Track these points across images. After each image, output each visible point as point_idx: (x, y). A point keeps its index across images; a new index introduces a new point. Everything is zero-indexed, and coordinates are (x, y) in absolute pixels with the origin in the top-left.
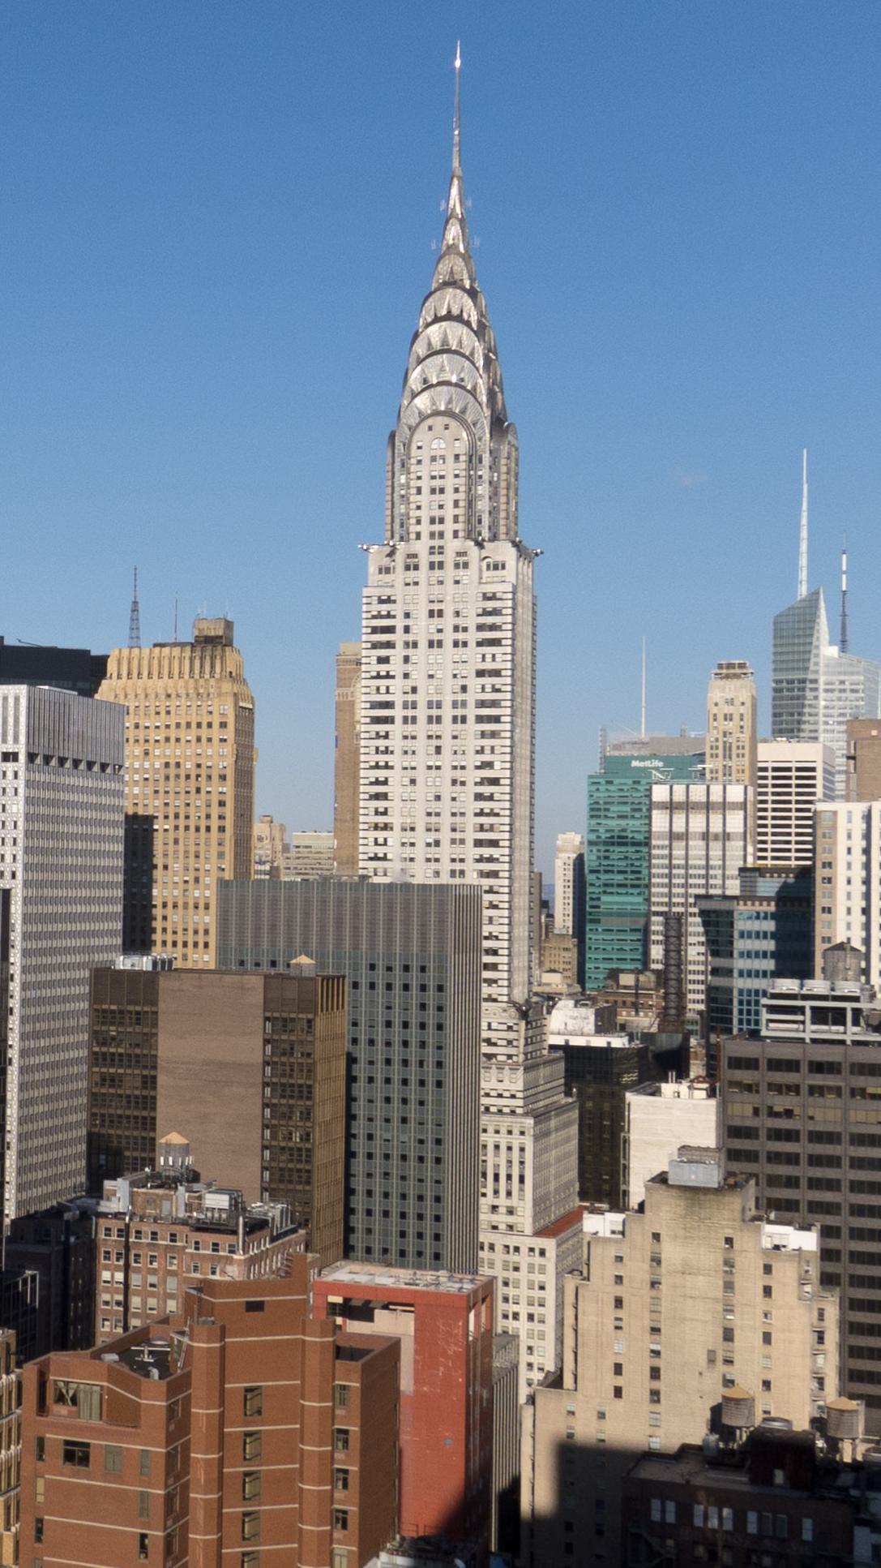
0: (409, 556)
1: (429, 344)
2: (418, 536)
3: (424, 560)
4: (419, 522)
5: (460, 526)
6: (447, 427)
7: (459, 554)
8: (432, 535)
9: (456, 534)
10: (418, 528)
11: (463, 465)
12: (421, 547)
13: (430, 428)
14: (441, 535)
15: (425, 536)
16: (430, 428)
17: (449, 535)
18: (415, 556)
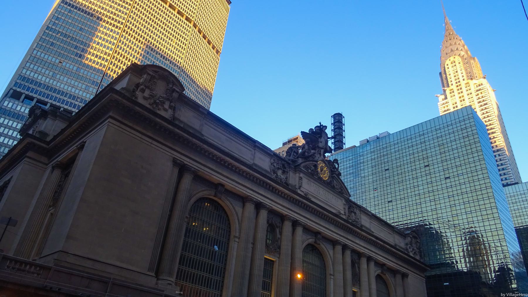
2: (452, 85)
3: (455, 89)
5: (465, 77)
7: (466, 84)
9: (464, 80)
12: (454, 87)
14: (459, 82)
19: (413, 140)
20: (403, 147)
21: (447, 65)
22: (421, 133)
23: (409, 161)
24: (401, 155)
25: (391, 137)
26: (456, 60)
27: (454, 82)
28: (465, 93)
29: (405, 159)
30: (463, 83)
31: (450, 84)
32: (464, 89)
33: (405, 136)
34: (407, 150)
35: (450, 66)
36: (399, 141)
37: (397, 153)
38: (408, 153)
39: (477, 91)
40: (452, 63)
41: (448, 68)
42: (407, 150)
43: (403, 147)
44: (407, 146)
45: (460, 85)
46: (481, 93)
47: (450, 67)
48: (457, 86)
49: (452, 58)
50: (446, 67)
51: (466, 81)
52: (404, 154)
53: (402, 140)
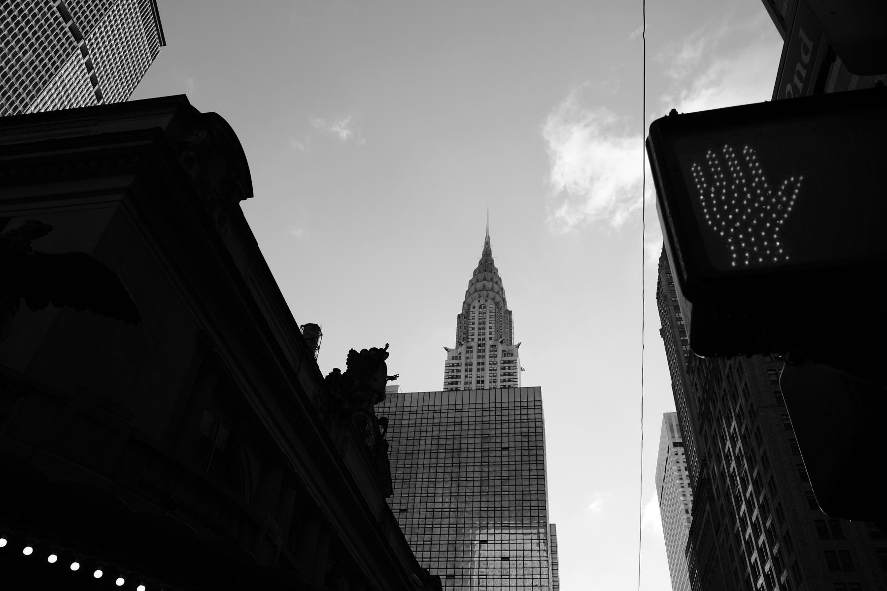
2: (473, 340)
7: (491, 346)
8: (479, 340)
12: (474, 344)
14: (484, 339)
15: (476, 340)
17: (487, 339)
19: (443, 415)
20: (424, 421)
21: (474, 307)
22: (458, 407)
23: (428, 447)
24: (417, 434)
25: (408, 399)
27: (476, 337)
28: (487, 360)
29: (422, 442)
30: (489, 343)
32: (487, 353)
33: (432, 403)
34: (430, 429)
35: (477, 310)
36: (420, 409)
37: (412, 429)
38: (429, 434)
39: (505, 362)
40: (480, 307)
42: (430, 429)
43: (424, 421)
44: (430, 421)
45: (483, 345)
46: (509, 368)
51: (491, 343)
52: (423, 434)
53: (426, 408)
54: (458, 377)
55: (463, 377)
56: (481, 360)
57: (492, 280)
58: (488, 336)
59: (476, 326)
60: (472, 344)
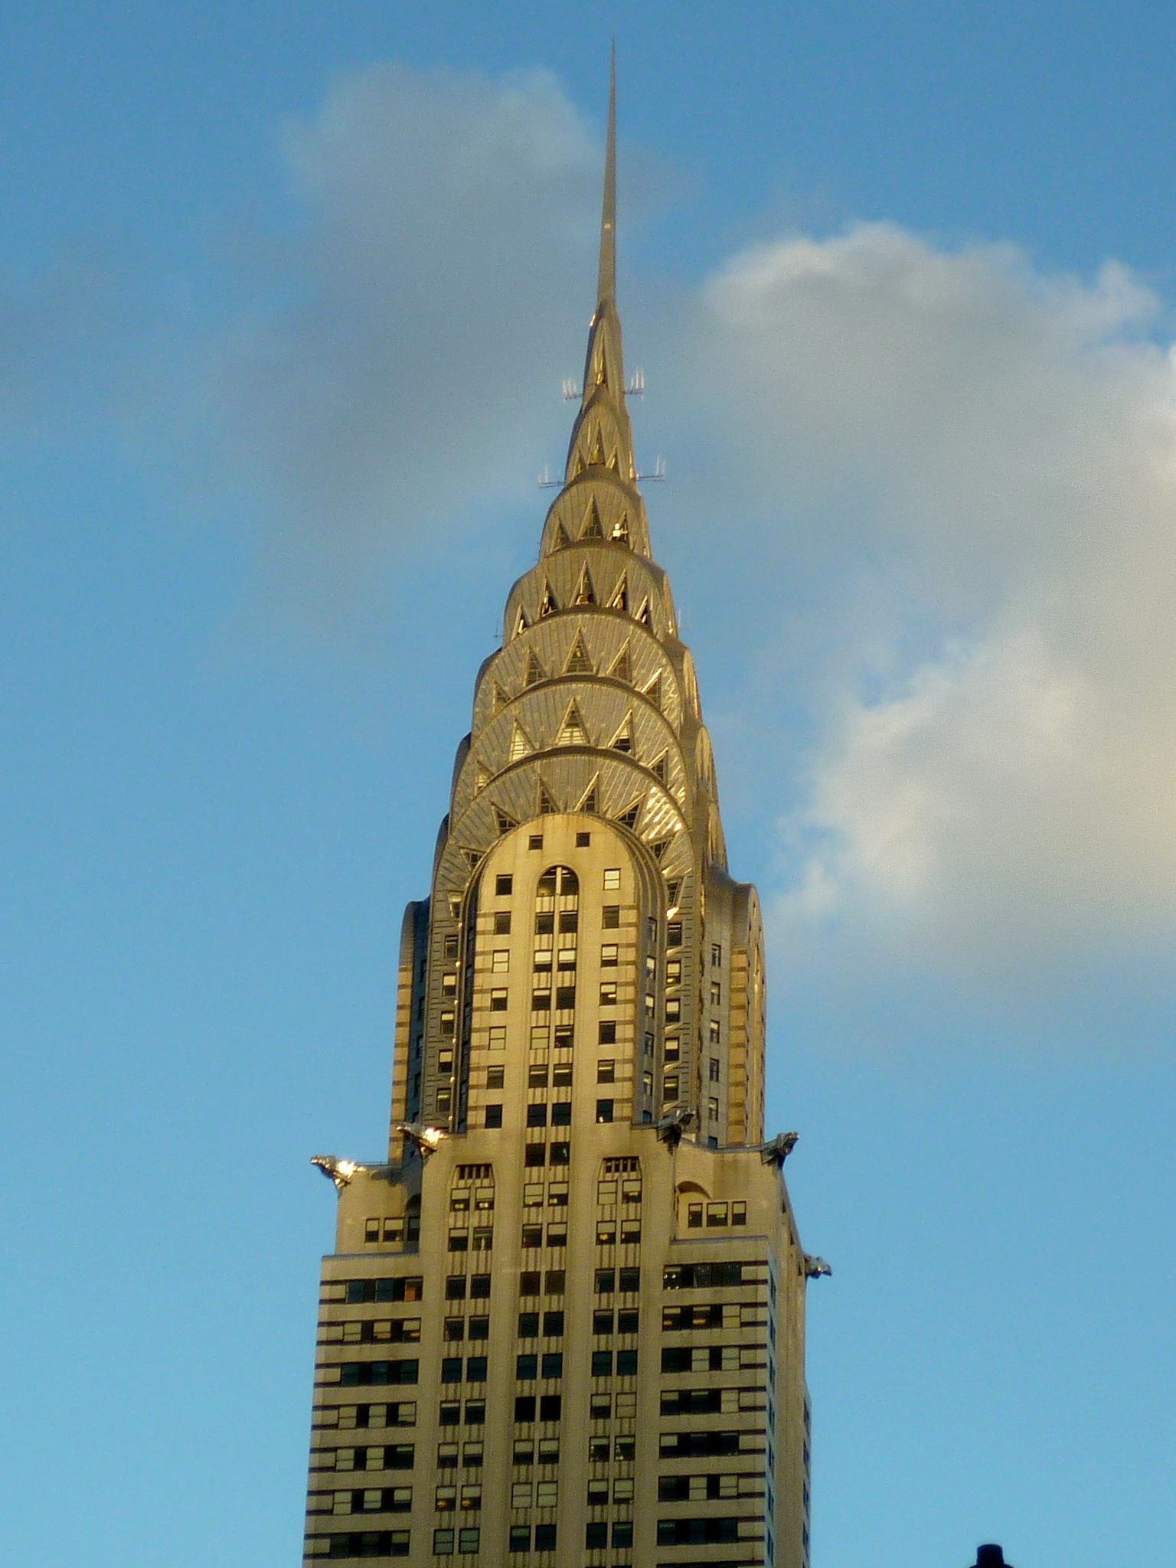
0: (467, 1170)
1: (534, 664)
2: (494, 1116)
4: (496, 1080)
6: (583, 840)
8: (536, 1115)
9: (605, 1109)
10: (494, 1097)
11: (630, 934)
12: (501, 1147)
13: (536, 843)
14: (563, 1114)
15: (514, 1117)
16: (536, 843)
17: (584, 1112)
18: (483, 1170)
21: (504, 886)
26: (584, 862)
27: (515, 1098)
31: (480, 1097)
40: (546, 881)
41: (503, 925)
45: (561, 1154)
47: (522, 923)
48: (534, 1156)
49: (558, 830)
50: (490, 901)
54: (402, 1372)
55: (430, 1371)
56: (543, 1260)
57: (625, 665)
58: (586, 1093)
59: (519, 1015)
60: (488, 1144)
